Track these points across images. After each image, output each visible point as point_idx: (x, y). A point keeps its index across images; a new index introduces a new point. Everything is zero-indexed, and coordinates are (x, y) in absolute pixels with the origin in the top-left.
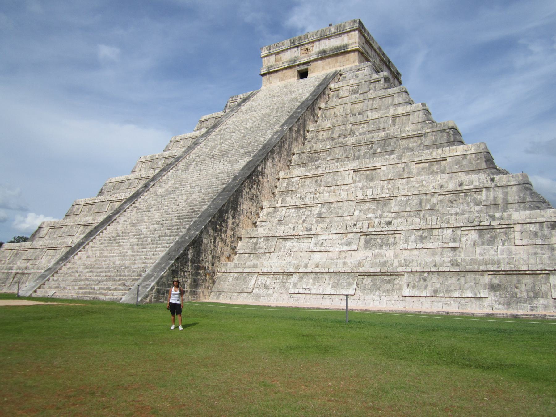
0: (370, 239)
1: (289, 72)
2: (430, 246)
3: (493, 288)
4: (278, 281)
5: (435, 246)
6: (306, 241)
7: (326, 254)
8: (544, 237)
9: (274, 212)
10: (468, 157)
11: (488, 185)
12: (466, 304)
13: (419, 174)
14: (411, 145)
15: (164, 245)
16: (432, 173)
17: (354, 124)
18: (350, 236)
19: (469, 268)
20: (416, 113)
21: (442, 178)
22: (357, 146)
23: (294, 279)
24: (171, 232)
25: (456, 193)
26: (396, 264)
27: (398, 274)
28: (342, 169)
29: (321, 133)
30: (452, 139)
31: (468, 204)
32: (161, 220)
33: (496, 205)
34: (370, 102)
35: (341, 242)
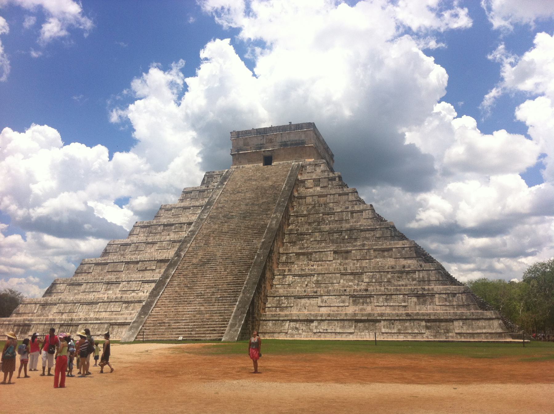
0: (356, 298)
2: (392, 304)
3: (427, 328)
5: (394, 304)
6: (314, 299)
7: (329, 308)
8: (450, 301)
9: (283, 278)
11: (419, 269)
12: (415, 336)
13: (376, 257)
14: (367, 235)
16: (384, 257)
17: (324, 214)
18: (343, 297)
19: (415, 317)
20: (367, 211)
21: (390, 262)
22: (331, 232)
23: (315, 324)
25: (401, 272)
28: (325, 250)
29: (300, 218)
30: (393, 235)
31: (408, 279)
33: (424, 281)
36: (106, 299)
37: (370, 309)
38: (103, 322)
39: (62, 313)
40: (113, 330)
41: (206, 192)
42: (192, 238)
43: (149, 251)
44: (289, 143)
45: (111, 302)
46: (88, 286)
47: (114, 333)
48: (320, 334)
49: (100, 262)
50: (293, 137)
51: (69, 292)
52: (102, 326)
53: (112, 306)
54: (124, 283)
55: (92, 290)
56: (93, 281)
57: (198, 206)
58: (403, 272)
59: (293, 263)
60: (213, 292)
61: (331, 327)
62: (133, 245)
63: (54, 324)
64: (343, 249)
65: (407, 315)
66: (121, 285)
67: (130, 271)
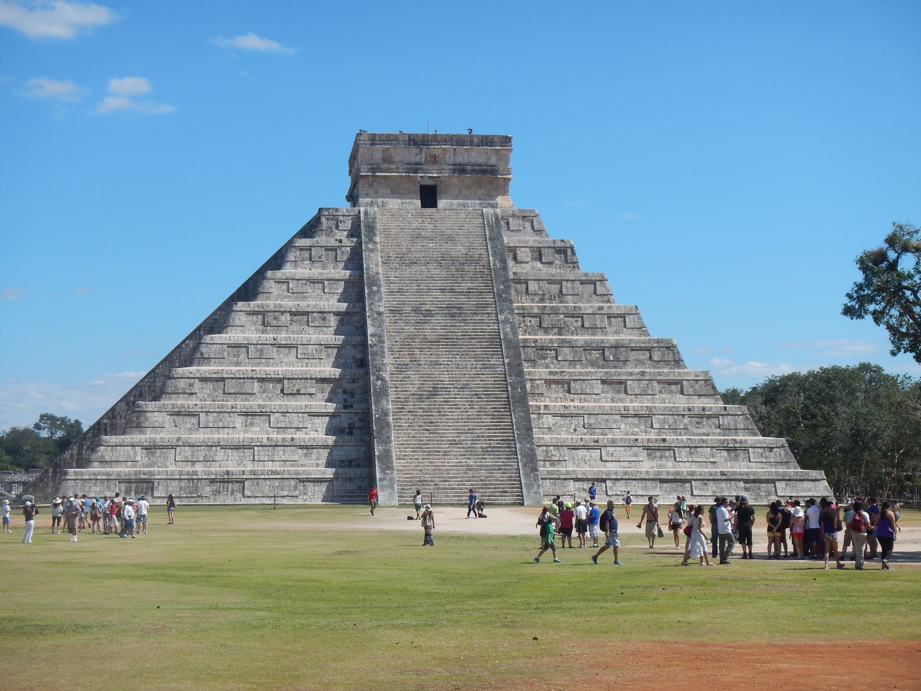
5: (701, 460)
8: (766, 458)
13: (661, 392)
14: (640, 357)
16: (671, 392)
19: (732, 477)
23: (609, 483)
29: (529, 319)
31: (710, 426)
36: (265, 441)
42: (383, 347)
43: (286, 360)
44: (468, 168)
45: (276, 446)
50: (476, 156)
52: (285, 483)
55: (220, 425)
56: (217, 410)
57: (338, 280)
58: (702, 416)
62: (251, 348)
63: (198, 479)
65: (722, 473)
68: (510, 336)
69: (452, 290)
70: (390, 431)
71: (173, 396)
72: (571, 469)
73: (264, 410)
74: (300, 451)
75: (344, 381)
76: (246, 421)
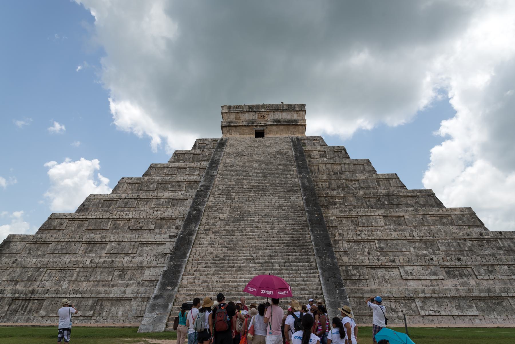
1: (247, 130)
2: (500, 277)
4: (402, 305)
6: (394, 270)
7: (420, 282)
10: (466, 216)
13: (434, 224)
15: (307, 271)
16: (444, 224)
17: (347, 180)
23: (419, 303)
24: (296, 259)
26: (498, 291)
27: (503, 299)
31: (492, 248)
32: (265, 245)
34: (346, 166)
35: (427, 272)
36: (88, 263)
37: (474, 283)
38: (85, 296)
39: (17, 282)
40: (102, 309)
41: (201, 156)
42: (207, 192)
43: (142, 209)
46: (59, 247)
47: (104, 314)
48: (431, 317)
49: (77, 217)
50: (286, 116)
51: (29, 253)
53: (99, 273)
54: (113, 244)
55: (64, 252)
59: (336, 228)
60: (270, 256)
61: (443, 309)
64: (393, 214)
66: (108, 246)
67: (120, 230)
68: (307, 184)
69: (267, 165)
70: (189, 248)
71: (46, 232)
72: (374, 287)
73: (104, 240)
74: (116, 273)
75: (178, 220)
76: (87, 249)
